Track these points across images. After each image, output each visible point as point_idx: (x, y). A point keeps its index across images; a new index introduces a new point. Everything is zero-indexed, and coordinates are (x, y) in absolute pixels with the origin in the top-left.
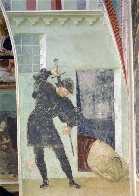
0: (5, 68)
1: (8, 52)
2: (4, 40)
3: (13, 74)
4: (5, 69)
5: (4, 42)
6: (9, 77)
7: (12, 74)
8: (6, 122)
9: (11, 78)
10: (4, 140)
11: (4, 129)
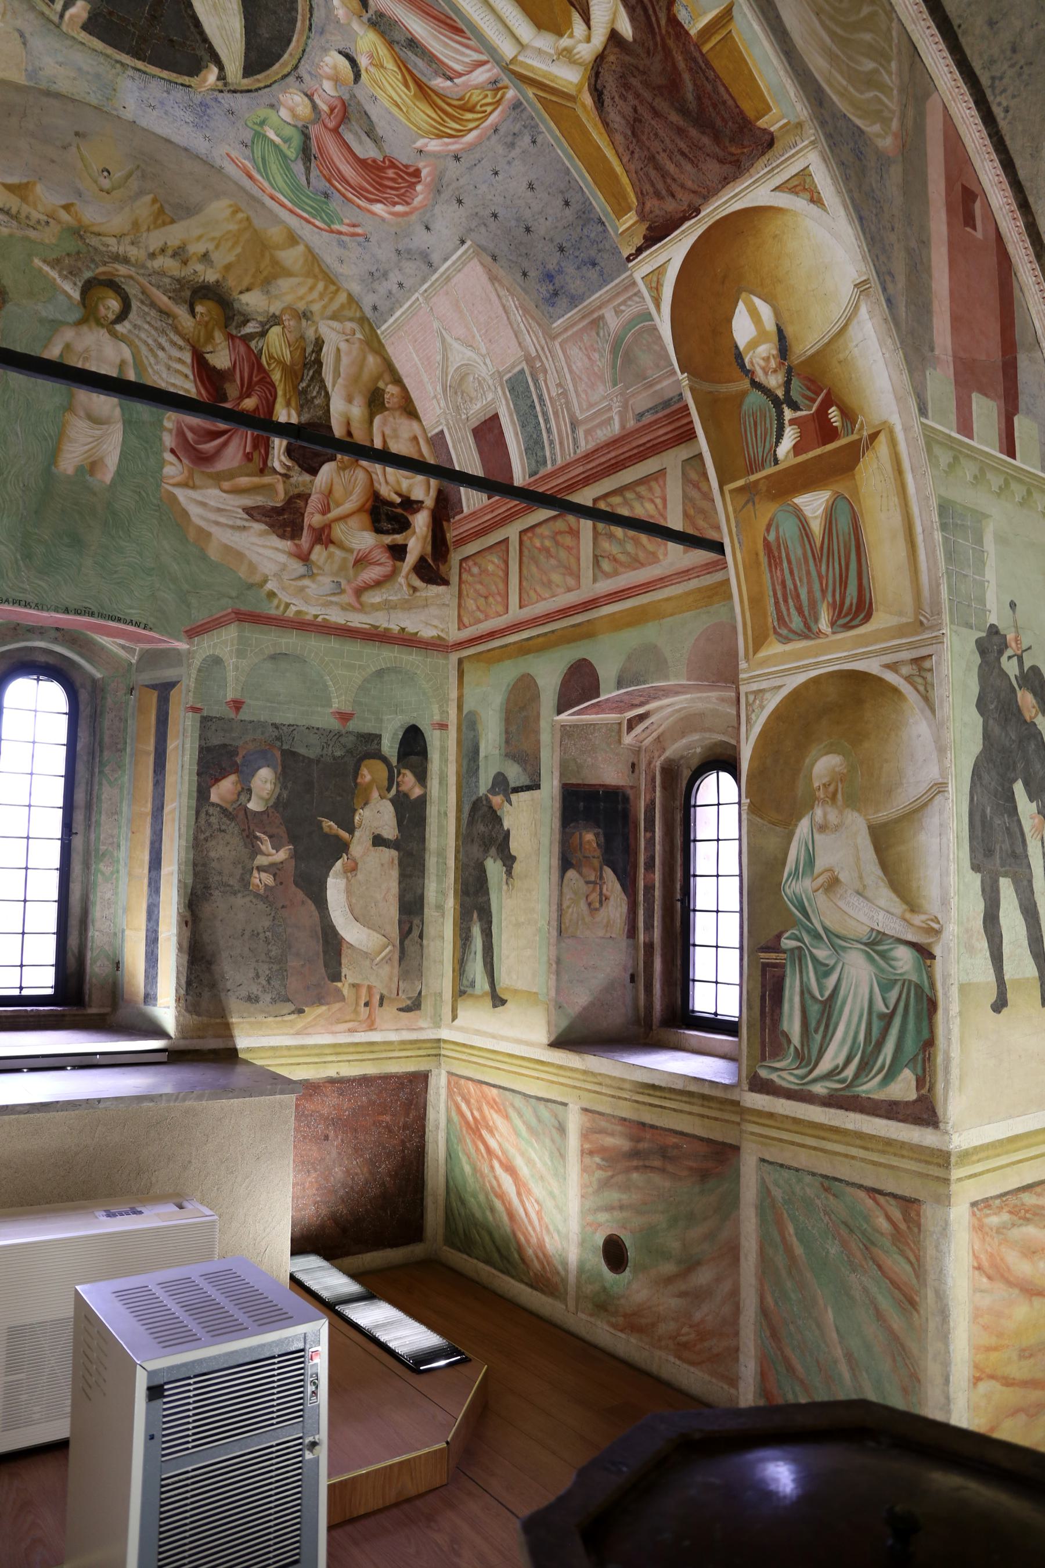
0: (289, 543)
3: (318, 574)
4: (287, 545)
7: (315, 571)
8: (275, 769)
9: (308, 587)
10: (263, 848)
11: (267, 800)
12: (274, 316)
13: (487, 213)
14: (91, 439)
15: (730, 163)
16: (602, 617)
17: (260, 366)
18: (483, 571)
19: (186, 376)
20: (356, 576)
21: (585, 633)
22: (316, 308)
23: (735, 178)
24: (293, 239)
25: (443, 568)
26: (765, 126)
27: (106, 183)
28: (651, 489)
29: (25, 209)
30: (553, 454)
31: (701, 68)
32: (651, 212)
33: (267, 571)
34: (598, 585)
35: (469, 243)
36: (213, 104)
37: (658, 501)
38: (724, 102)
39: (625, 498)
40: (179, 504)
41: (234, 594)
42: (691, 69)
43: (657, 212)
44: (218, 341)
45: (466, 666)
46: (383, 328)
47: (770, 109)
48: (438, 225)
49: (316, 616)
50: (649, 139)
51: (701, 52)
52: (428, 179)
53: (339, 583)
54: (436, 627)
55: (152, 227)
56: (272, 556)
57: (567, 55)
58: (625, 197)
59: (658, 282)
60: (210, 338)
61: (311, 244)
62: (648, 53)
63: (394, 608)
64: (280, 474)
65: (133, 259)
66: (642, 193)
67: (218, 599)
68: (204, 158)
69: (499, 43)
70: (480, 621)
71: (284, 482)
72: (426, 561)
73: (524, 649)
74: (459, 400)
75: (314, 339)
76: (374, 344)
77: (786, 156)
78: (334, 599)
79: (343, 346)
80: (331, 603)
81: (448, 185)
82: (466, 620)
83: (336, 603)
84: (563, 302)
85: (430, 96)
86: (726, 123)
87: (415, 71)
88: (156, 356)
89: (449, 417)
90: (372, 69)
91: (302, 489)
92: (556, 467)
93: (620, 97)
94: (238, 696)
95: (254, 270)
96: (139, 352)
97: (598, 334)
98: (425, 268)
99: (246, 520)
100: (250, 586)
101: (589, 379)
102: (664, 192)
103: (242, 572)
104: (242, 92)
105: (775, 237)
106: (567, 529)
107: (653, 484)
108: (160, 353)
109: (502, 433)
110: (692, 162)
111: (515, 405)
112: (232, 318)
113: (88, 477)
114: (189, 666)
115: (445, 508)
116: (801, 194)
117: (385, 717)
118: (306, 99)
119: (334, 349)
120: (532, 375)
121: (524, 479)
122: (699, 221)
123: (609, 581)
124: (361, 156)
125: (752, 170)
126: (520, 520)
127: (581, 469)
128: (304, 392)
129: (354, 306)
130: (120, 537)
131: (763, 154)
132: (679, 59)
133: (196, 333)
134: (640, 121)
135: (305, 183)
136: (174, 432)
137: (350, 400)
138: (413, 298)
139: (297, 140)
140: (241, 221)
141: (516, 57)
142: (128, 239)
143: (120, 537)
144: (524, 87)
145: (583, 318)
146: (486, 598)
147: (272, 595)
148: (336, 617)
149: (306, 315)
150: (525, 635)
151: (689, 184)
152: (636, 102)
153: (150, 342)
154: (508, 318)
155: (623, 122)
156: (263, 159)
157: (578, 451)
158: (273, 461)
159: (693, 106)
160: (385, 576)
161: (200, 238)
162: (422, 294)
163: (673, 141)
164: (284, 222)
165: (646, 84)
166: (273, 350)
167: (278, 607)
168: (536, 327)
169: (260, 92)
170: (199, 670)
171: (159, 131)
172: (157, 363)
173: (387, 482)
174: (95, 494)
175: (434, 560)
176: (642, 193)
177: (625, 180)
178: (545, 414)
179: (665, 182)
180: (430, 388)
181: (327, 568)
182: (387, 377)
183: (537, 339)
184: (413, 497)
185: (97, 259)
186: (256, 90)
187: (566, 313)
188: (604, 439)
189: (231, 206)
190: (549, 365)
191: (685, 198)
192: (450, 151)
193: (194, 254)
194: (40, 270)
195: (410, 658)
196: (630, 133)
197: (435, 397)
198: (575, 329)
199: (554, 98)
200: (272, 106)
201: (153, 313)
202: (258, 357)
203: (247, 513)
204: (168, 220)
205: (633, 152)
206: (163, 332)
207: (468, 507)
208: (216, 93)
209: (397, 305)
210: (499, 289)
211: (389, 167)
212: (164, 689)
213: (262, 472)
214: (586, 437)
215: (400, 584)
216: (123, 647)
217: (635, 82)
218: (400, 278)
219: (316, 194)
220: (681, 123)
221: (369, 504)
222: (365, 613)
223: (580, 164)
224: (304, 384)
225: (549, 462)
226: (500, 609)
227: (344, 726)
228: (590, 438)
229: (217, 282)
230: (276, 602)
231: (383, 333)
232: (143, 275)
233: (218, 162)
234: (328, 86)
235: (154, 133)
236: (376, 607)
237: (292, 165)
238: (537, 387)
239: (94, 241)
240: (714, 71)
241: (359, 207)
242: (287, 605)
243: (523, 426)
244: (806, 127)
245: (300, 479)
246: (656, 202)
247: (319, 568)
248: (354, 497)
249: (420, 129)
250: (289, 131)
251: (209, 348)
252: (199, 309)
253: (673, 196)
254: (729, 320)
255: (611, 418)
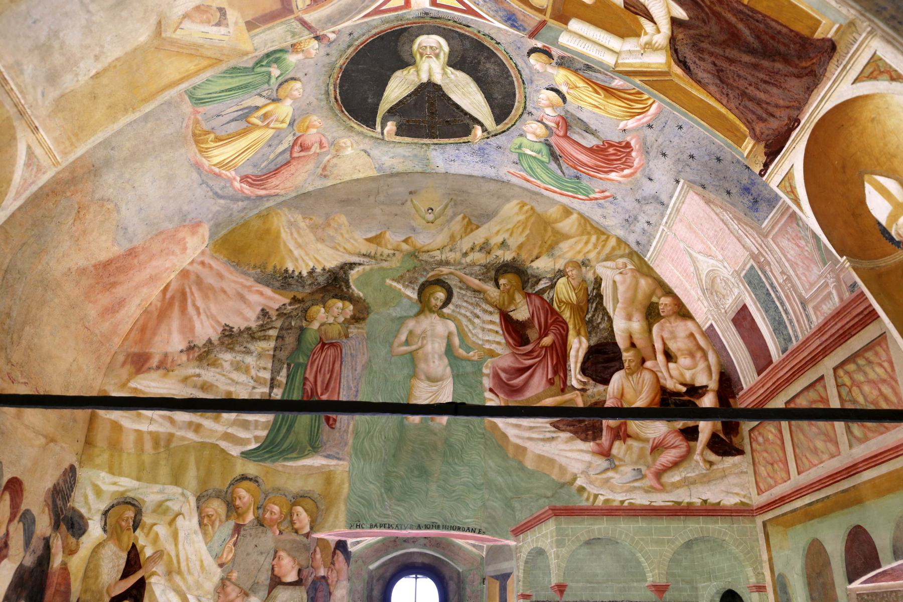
0: (592, 444)
1: (599, 391)
2: (584, 352)
4: (590, 445)
5: (584, 358)
6: (605, 476)
7: (617, 463)
9: (612, 478)
12: (560, 271)
13: (686, 156)
14: (431, 394)
15: (807, 75)
16: (865, 483)
17: (553, 311)
18: (767, 440)
19: (497, 332)
20: (654, 461)
21: (851, 499)
22: (592, 256)
23: (816, 85)
24: (567, 212)
25: (735, 440)
26: (822, 36)
27: (430, 217)
28: (877, 354)
29: (380, 250)
30: (795, 331)
31: (748, 15)
32: (762, 133)
33: (575, 471)
34: (854, 451)
35: (682, 181)
36: (486, 146)
37: (886, 364)
38: (779, 32)
39: (857, 365)
40: (499, 429)
41: (549, 494)
42: (742, 20)
43: (767, 132)
44: (518, 301)
45: (770, 529)
46: (648, 256)
47: (819, 22)
48: (656, 175)
49: (622, 502)
50: (734, 80)
51: (743, 4)
52: (637, 146)
53: (639, 470)
54: (737, 494)
55: (463, 235)
56: (579, 457)
57: (649, 47)
58: (738, 129)
59: (791, 186)
60: (512, 299)
61: (581, 211)
62: (704, 22)
63: (694, 483)
64: (578, 390)
65: (452, 261)
66: (749, 122)
67: (537, 500)
68: (496, 178)
69: (602, 57)
70: (771, 487)
71: (582, 395)
72: (718, 436)
73: (809, 514)
74: (716, 298)
75: (593, 279)
76: (644, 269)
77: (852, 52)
78: (637, 484)
79: (618, 278)
80: (635, 488)
81: (651, 146)
82: (761, 485)
83: (639, 488)
84: (763, 206)
85: (615, 93)
86: (789, 47)
87: (598, 82)
88: (473, 323)
89: (713, 313)
90: (571, 91)
91: (597, 397)
92: (800, 342)
93: (699, 60)
94: (561, 580)
95: (540, 242)
96: (461, 323)
97: (798, 225)
98: (660, 207)
99: (554, 432)
100: (563, 485)
101: (804, 263)
102: (764, 116)
103: (555, 475)
104: (500, 134)
105: (873, 120)
106: (819, 399)
107: (878, 349)
108: (476, 321)
109: (753, 320)
110: (776, 86)
111: (756, 295)
112: (528, 281)
113: (430, 423)
114: (518, 559)
115: (730, 386)
116: (880, 78)
117: (700, 585)
118: (539, 124)
119: (611, 282)
120: (760, 269)
121: (779, 356)
122: (803, 128)
123: (863, 446)
124: (588, 146)
125: (827, 74)
126: (783, 393)
127: (818, 342)
128: (591, 321)
129: (623, 246)
130: (456, 464)
131: (831, 58)
132: (729, 16)
133: (502, 299)
134: (722, 71)
135: (561, 174)
136: (491, 376)
137: (629, 318)
138: (660, 230)
139: (545, 150)
140: (527, 212)
141: (617, 61)
142: (448, 249)
143: (456, 464)
144: (632, 78)
145: (782, 214)
146: (772, 464)
147: (581, 489)
148: (641, 499)
149: (585, 263)
150: (807, 500)
151: (781, 103)
152: (713, 59)
153: (468, 314)
154: (729, 229)
155: (709, 76)
156: (530, 167)
157: (813, 326)
158: (571, 380)
159: (756, 44)
160: (681, 457)
161: (498, 231)
162: (665, 226)
163: (753, 75)
164: (559, 202)
165: (713, 43)
166: (561, 296)
167: (588, 499)
168: (751, 231)
169: (511, 130)
170: (526, 562)
171: (463, 172)
172: (475, 328)
173: (671, 377)
174: (435, 434)
175: (726, 434)
176: (749, 122)
177: (731, 116)
178: (779, 298)
179: (762, 108)
180: (693, 293)
181: (627, 459)
182: (659, 292)
183: (755, 239)
184: (698, 384)
185: (427, 268)
186: (508, 129)
187: (769, 214)
188: (829, 312)
189: (519, 203)
190: (770, 258)
191: (783, 114)
192: (643, 123)
193: (495, 244)
194: (391, 285)
195: (717, 526)
196: (719, 82)
197: (699, 299)
198: (779, 225)
199: (655, 78)
200: (521, 135)
201: (469, 293)
202: (550, 305)
203: (554, 426)
204: (474, 227)
205: (727, 95)
206: (478, 305)
207: (746, 384)
208: (486, 140)
209: (652, 237)
210: (714, 208)
211: (609, 147)
212: (504, 578)
213: (563, 391)
214: (815, 313)
215: (697, 461)
216: (474, 546)
217: (704, 45)
218: (646, 218)
219: (571, 179)
220: (753, 60)
221: (658, 398)
222: (667, 492)
223: (693, 116)
224: (589, 316)
225: (793, 339)
226: (784, 475)
227: (661, 598)
228: (819, 313)
229: (514, 258)
230: (585, 495)
231: (649, 260)
232: (460, 269)
233: (505, 179)
234: (549, 111)
235: (460, 175)
236: (676, 486)
237: (549, 166)
238: (768, 278)
239: (425, 257)
240: (760, 13)
241: (601, 178)
242: (596, 496)
243: (766, 312)
244: (858, 23)
245: (595, 390)
246: (762, 125)
247: (620, 460)
248: (643, 395)
249: (618, 116)
250: (538, 146)
251: (512, 308)
252: (502, 281)
253: (773, 116)
254: (862, 201)
255: (830, 293)
